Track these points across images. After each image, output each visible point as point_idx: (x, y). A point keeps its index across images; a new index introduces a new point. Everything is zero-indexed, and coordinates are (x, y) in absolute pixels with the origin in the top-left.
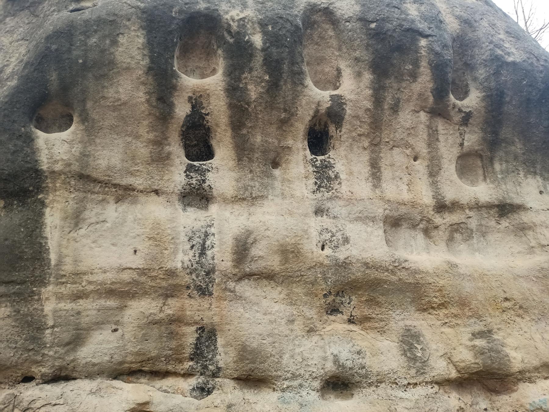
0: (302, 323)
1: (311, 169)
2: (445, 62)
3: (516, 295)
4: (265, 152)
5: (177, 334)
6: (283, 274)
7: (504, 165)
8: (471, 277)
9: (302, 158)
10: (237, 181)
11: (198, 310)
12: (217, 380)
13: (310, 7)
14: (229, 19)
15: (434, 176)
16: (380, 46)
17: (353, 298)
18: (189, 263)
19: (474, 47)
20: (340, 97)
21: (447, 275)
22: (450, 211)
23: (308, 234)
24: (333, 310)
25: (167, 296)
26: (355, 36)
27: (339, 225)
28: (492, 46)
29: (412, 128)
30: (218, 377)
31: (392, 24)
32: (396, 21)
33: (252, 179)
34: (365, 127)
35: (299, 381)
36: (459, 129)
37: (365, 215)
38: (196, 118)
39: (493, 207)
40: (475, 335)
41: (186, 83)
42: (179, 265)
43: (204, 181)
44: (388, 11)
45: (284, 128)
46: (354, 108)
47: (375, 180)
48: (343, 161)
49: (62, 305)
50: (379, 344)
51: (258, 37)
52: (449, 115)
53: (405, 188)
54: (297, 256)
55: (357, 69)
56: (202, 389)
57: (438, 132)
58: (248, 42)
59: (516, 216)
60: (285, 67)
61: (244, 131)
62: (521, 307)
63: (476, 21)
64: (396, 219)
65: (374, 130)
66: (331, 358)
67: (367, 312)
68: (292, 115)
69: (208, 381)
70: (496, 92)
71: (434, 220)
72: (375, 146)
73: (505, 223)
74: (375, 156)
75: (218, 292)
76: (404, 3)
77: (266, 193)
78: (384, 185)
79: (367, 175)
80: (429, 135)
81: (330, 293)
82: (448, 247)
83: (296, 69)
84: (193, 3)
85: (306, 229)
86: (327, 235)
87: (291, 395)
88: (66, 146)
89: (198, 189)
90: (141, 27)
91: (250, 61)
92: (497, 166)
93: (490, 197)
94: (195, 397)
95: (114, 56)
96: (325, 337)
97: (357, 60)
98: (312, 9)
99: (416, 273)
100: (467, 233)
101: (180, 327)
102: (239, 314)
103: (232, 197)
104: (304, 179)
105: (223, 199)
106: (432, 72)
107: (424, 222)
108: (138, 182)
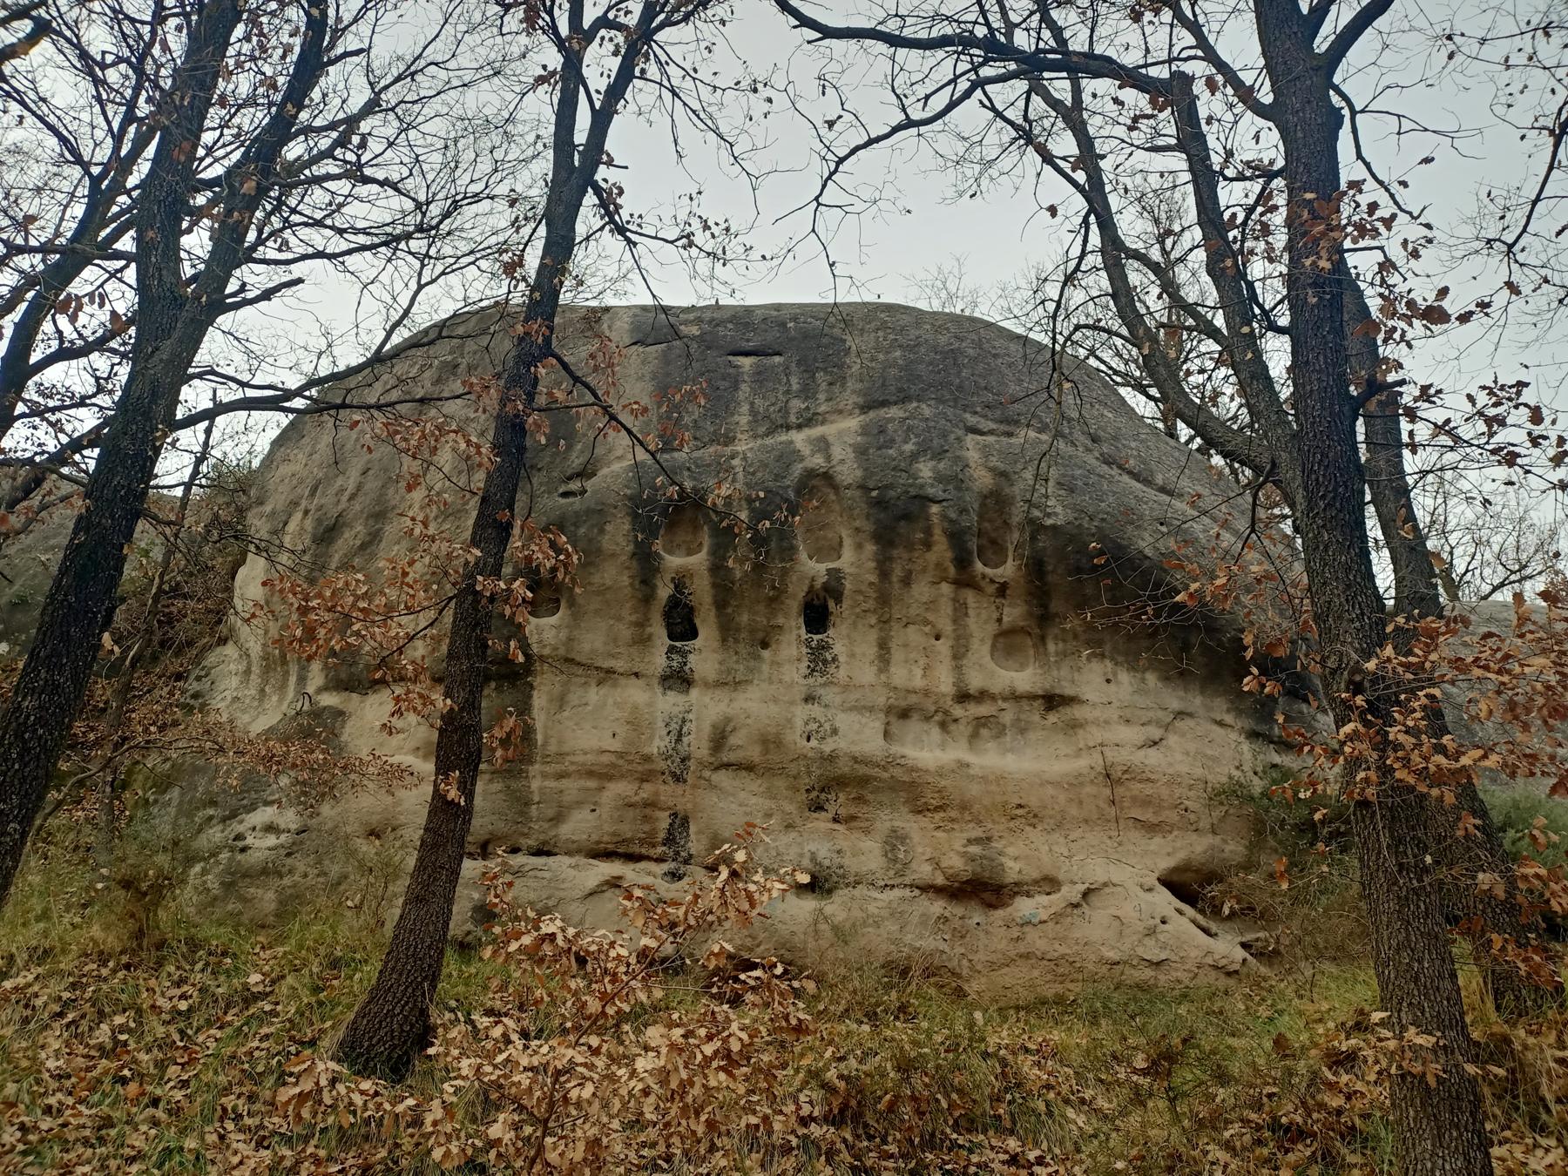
1: (805, 650)
3: (1033, 802)
4: (752, 631)
7: (1061, 645)
8: (984, 779)
20: (838, 570)
24: (819, 808)
25: (643, 781)
40: (970, 842)
49: (547, 783)
50: (862, 845)
53: (918, 672)
61: (729, 610)
62: (1035, 816)
66: (808, 855)
72: (885, 622)
73: (1053, 718)
78: (893, 669)
80: (955, 609)
88: (554, 631)
92: (1051, 647)
97: (857, 530)
108: (619, 665)
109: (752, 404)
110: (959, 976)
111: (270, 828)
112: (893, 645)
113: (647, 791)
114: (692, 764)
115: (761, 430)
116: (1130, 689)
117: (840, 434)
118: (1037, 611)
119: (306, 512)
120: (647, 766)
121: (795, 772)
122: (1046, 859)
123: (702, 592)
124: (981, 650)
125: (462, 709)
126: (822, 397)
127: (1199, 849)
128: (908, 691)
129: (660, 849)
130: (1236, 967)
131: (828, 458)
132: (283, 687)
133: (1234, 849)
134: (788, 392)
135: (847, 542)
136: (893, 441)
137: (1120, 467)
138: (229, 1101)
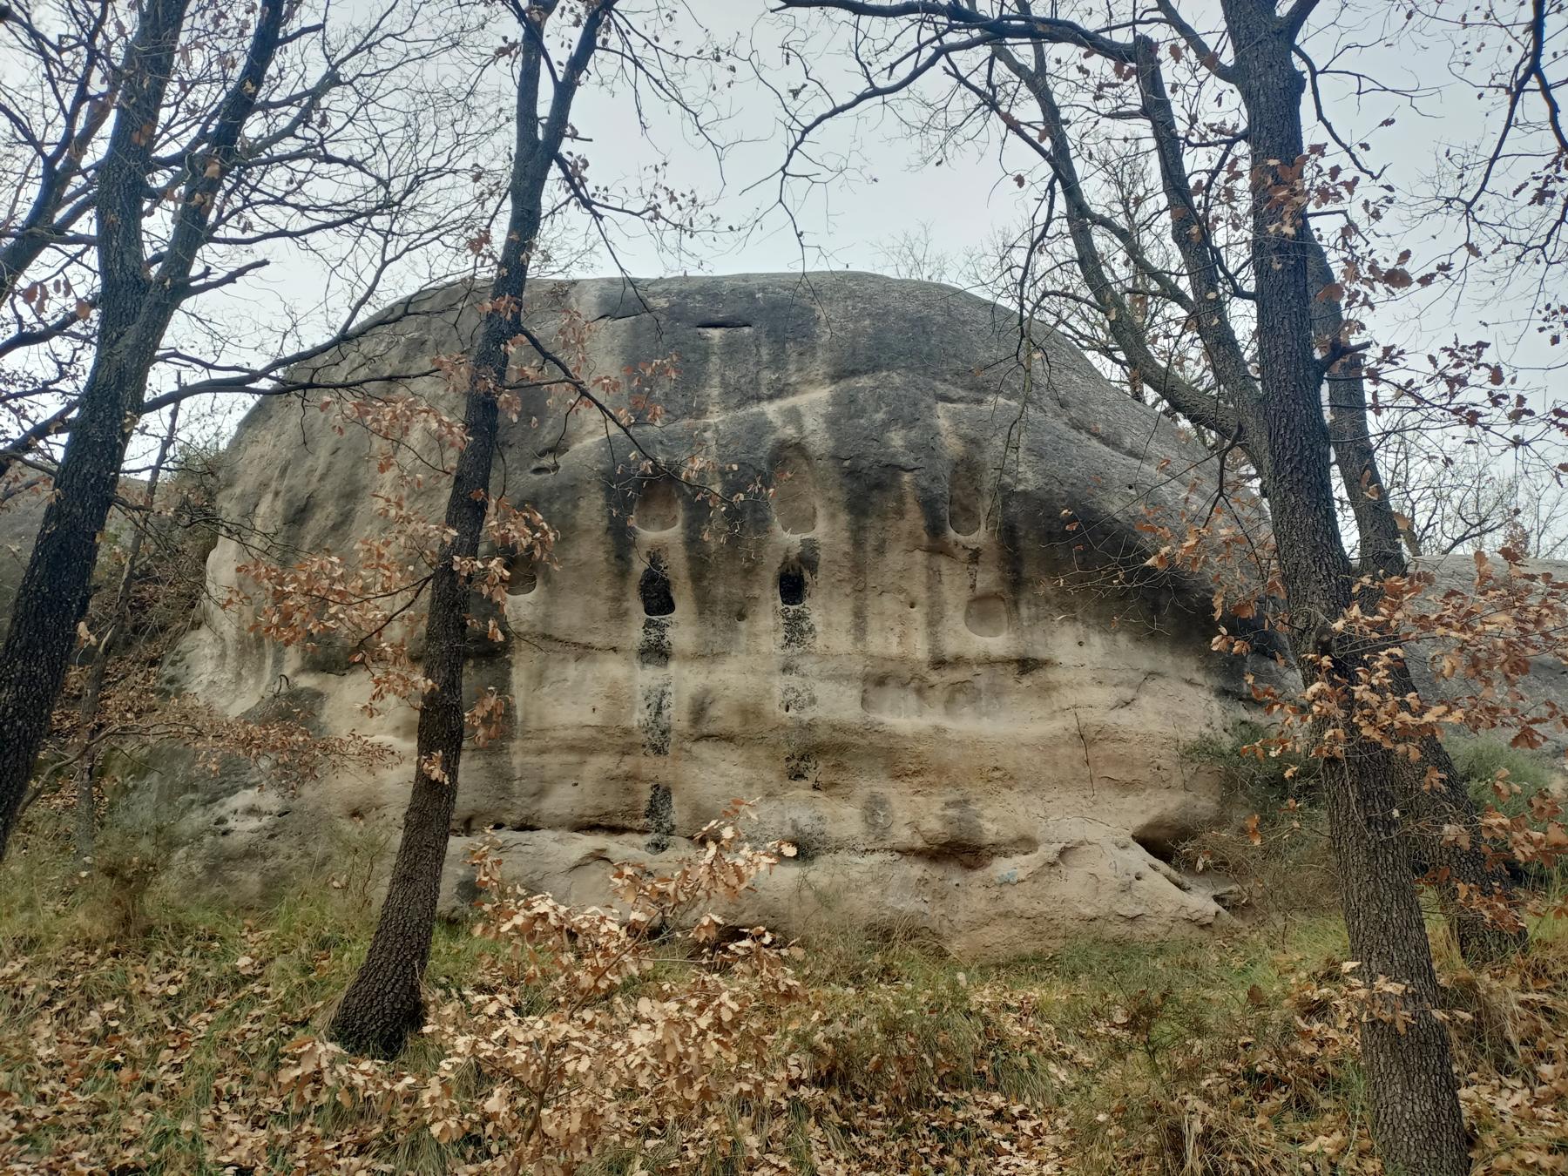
1: (781, 621)
3: (1009, 764)
4: (729, 603)
7: (1033, 609)
10: (698, 636)
20: (812, 541)
24: (799, 776)
25: (624, 754)
49: (528, 759)
53: (895, 640)
56: (657, 846)
59: (1041, 672)
61: (705, 583)
72: (860, 591)
73: (1027, 681)
78: (869, 638)
80: (929, 577)
92: (1024, 611)
108: (597, 640)
109: (723, 376)
110: (940, 936)
111: (252, 811)
113: (628, 764)
114: (673, 736)
116: (1102, 652)
117: (811, 405)
118: (1009, 576)
119: (277, 494)
120: (628, 740)
121: (774, 741)
122: (1022, 820)
123: (677, 565)
124: (955, 618)
125: (443, 689)
126: (792, 367)
127: (1171, 805)
130: (1209, 920)
131: (800, 428)
132: (259, 670)
133: (1205, 804)
134: (758, 363)
135: (821, 513)
137: (1088, 431)
138: (223, 1083)
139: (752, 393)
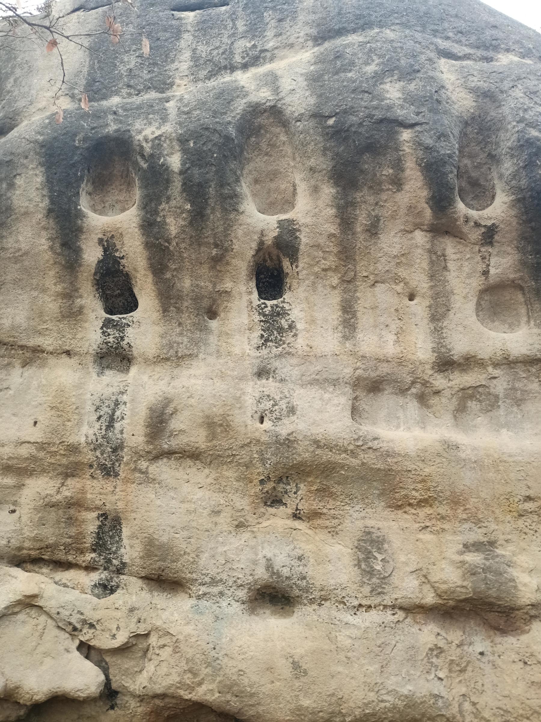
0: (230, 515)
1: (257, 318)
2: (442, 159)
4: (197, 299)
5: (77, 519)
6: (211, 453)
9: (246, 304)
10: (162, 337)
11: (100, 494)
12: (122, 577)
13: (251, 109)
14: (141, 139)
15: (438, 320)
16: (342, 148)
17: (302, 486)
18: (94, 438)
19: (498, 130)
20: (291, 222)
21: (438, 460)
22: (463, 369)
23: (240, 403)
25: (67, 476)
26: (308, 138)
27: (286, 391)
28: (521, 126)
29: (403, 254)
30: (124, 574)
31: (357, 116)
32: (364, 112)
33: (181, 334)
34: (331, 258)
35: (220, 588)
36: (480, 251)
37: (324, 376)
38: (109, 263)
39: (535, 362)
41: (93, 223)
42: (83, 440)
43: (122, 338)
44: (352, 99)
45: (218, 268)
46: (312, 234)
47: (346, 330)
48: (301, 306)
50: (328, 549)
51: (176, 158)
52: (461, 232)
53: (391, 338)
54: (226, 431)
55: (313, 182)
56: (105, 587)
57: (447, 258)
58: (163, 165)
60: (212, 191)
61: (168, 275)
63: (502, 92)
64: (374, 382)
65: (345, 261)
66: (263, 562)
67: (316, 505)
68: (226, 250)
69: (112, 578)
70: (529, 193)
71: (433, 382)
74: (348, 297)
75: (126, 472)
76: (381, 84)
77: (196, 351)
78: (360, 336)
79: (336, 322)
80: (432, 263)
81: (269, 478)
82: (456, 420)
83: (226, 192)
84: (101, 126)
85: (238, 395)
86: (268, 403)
87: (208, 604)
89: (116, 348)
90: (40, 163)
91: (167, 188)
93: (529, 347)
94: (98, 597)
95: (11, 200)
96: (258, 534)
97: (312, 169)
98: (254, 111)
99: (388, 456)
100: (489, 400)
101: (79, 512)
102: (148, 501)
103: (154, 357)
104: (247, 331)
105: (144, 359)
106: (423, 174)
107: (418, 386)
109: (194, 50)
112: (360, 307)
115: (203, 74)
126: (270, 34)
128: (379, 360)
129: (90, 556)
131: (276, 90)
134: (233, 35)
135: (302, 188)
136: (352, 63)
139: (223, 63)
